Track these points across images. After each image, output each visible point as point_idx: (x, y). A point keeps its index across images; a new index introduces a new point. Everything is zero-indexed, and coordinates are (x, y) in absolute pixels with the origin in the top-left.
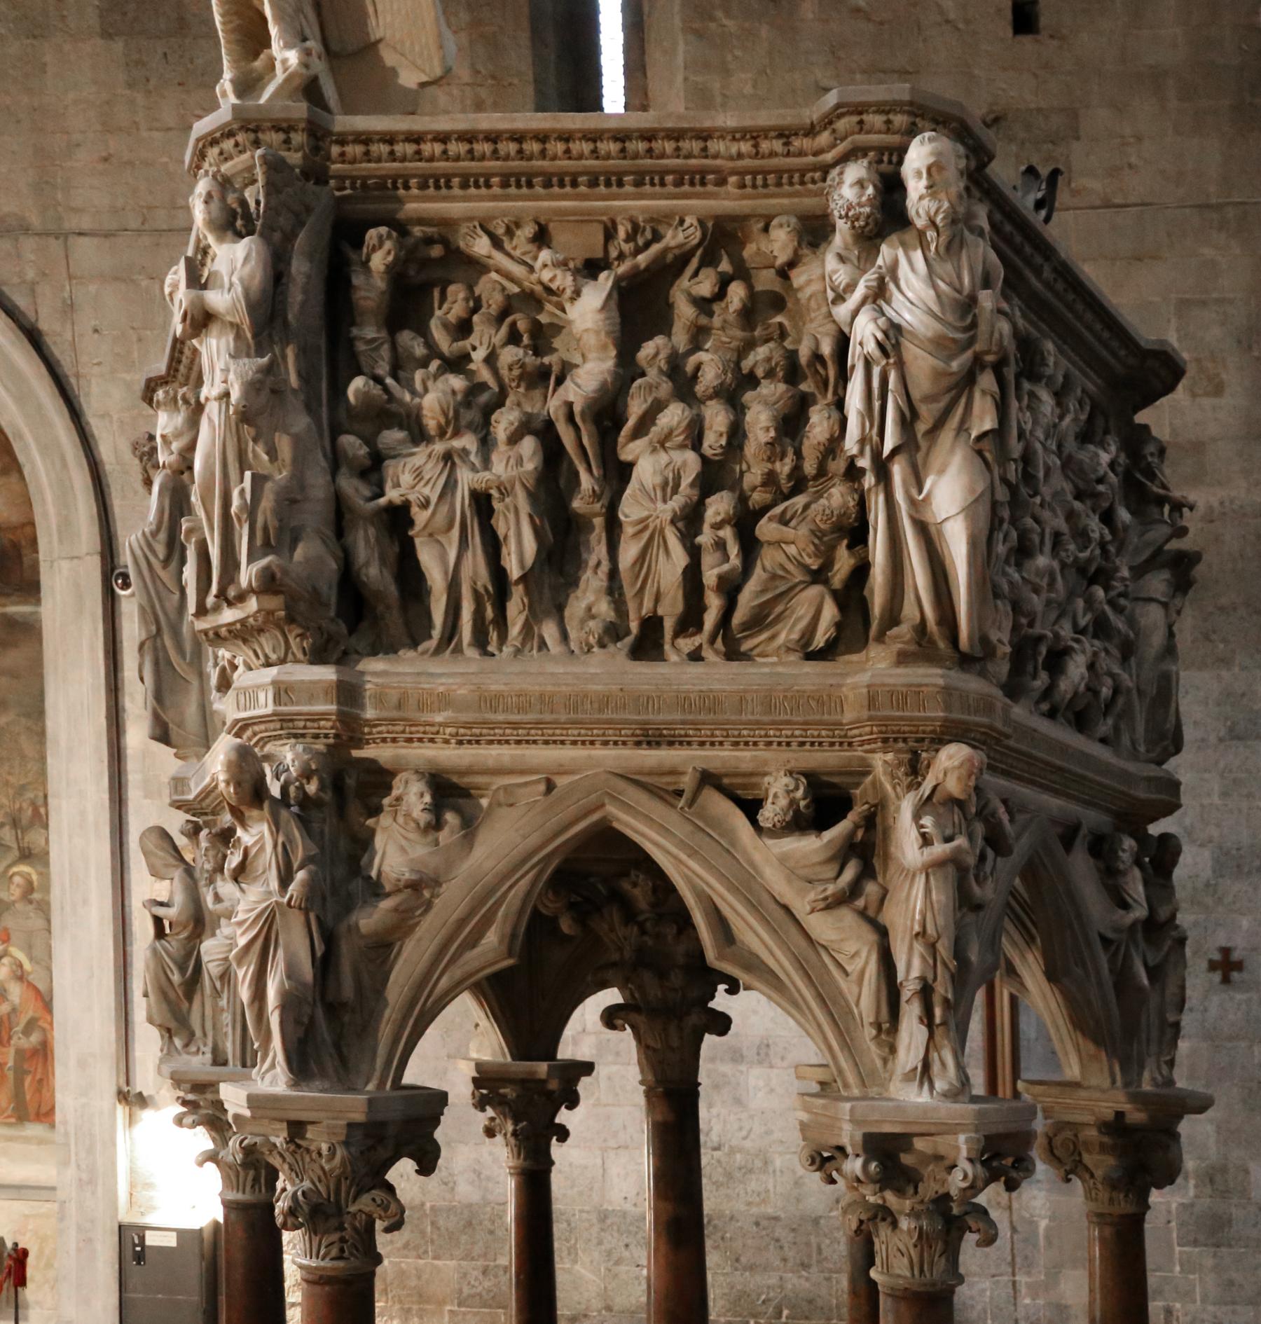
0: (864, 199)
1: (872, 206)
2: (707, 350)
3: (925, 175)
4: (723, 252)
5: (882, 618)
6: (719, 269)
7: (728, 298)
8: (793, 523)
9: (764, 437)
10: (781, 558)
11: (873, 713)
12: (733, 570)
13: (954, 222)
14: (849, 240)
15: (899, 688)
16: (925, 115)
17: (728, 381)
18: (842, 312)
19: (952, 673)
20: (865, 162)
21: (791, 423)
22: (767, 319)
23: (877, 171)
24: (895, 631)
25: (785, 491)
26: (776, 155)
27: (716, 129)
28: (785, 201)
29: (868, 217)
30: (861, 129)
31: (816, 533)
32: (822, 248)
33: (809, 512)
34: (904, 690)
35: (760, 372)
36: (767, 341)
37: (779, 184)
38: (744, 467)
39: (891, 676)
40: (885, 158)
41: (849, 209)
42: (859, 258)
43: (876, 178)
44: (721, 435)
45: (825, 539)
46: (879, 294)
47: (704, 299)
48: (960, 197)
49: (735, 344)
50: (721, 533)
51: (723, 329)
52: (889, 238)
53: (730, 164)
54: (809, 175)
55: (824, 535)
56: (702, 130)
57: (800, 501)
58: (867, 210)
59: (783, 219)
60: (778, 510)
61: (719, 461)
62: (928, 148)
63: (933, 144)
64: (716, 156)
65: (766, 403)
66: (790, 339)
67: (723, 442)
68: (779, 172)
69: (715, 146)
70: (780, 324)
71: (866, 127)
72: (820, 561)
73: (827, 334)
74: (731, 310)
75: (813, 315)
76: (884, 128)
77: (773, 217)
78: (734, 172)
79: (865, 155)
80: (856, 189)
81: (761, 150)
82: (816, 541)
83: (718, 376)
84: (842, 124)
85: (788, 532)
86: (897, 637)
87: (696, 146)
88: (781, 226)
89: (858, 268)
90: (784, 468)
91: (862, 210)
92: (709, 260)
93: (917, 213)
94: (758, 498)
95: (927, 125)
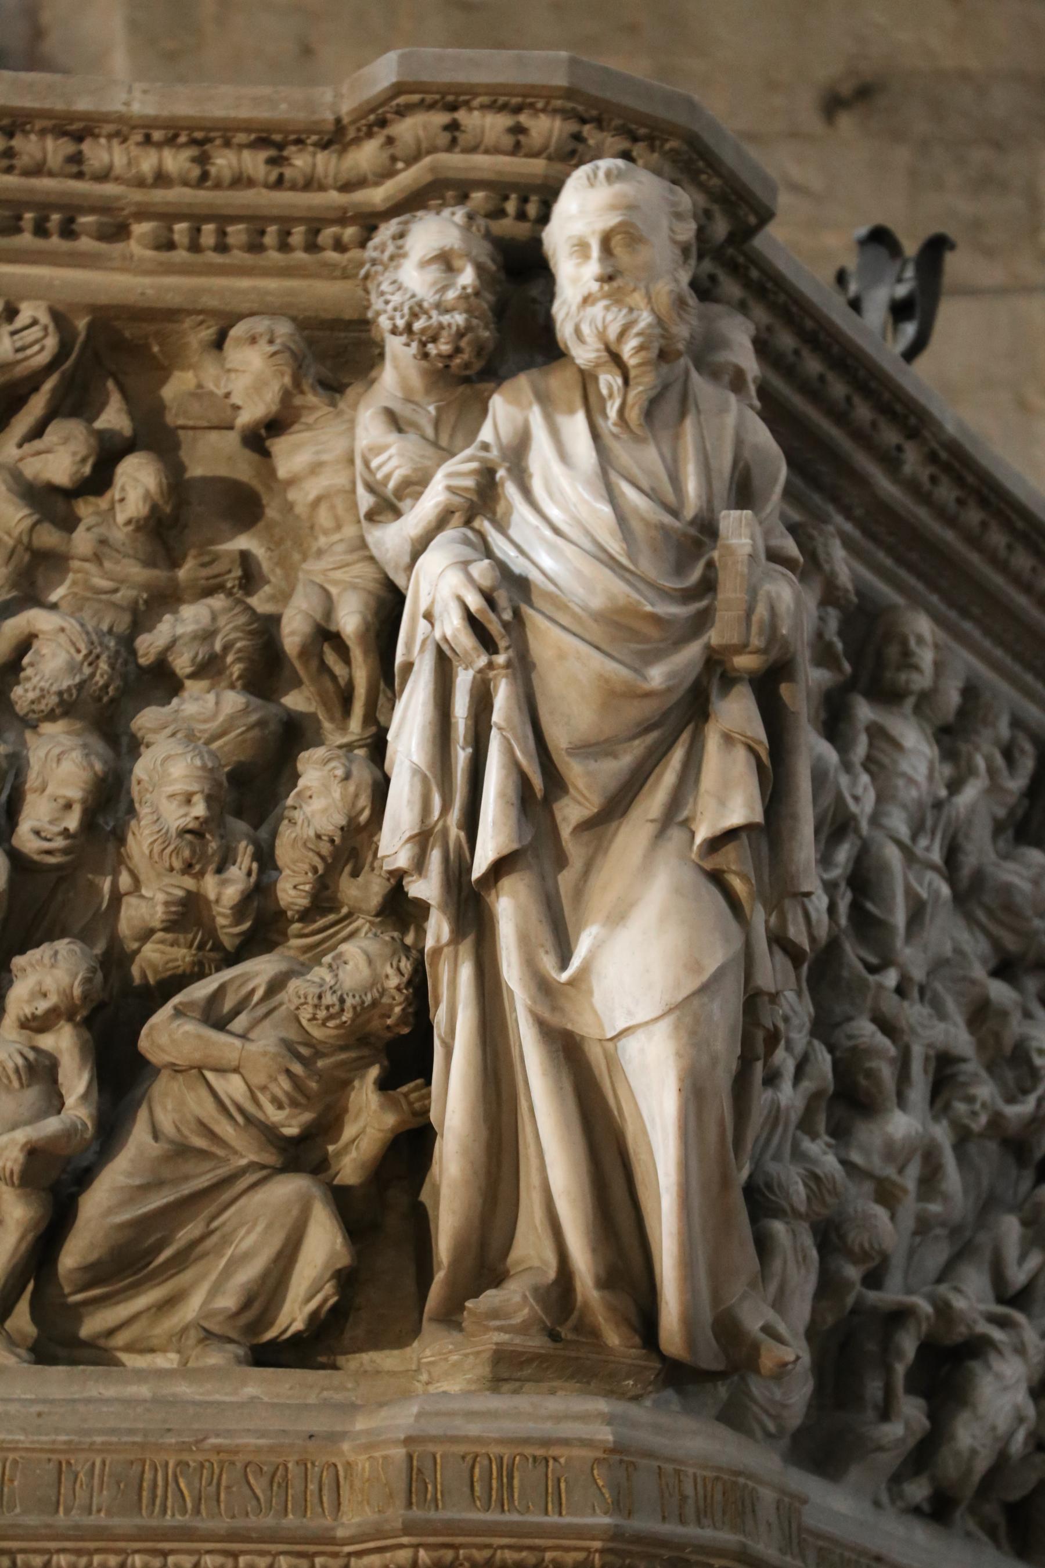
0: (451, 295)
1: (469, 311)
2: (54, 607)
3: (595, 251)
4: (110, 384)
5: (456, 1261)
6: (99, 424)
7: (115, 493)
8: (239, 1024)
9: (177, 817)
10: (208, 1110)
11: (417, 1513)
12: (70, 1133)
13: (664, 356)
14: (416, 381)
15: (494, 1450)
16: (599, 120)
17: (100, 680)
18: (391, 539)
19: (634, 1411)
20: (459, 215)
21: (251, 788)
22: (212, 542)
23: (488, 235)
24: (491, 1298)
25: (228, 943)
26: (251, 183)
27: (104, 118)
28: (272, 284)
29: (460, 334)
30: (454, 141)
31: (299, 1050)
32: (351, 392)
33: (282, 996)
34: (506, 1452)
35: (182, 663)
36: (209, 592)
37: (255, 247)
38: (125, 881)
39: (471, 1415)
40: (511, 206)
41: (414, 316)
42: (437, 424)
43: (483, 250)
44: (68, 806)
45: (320, 1064)
46: (481, 502)
47: (52, 489)
48: (680, 303)
49: (125, 595)
50: (47, 1041)
51: (97, 558)
52: (507, 385)
53: (137, 196)
54: (328, 233)
55: (318, 1054)
56: (71, 117)
57: (261, 968)
58: (459, 319)
59: (260, 325)
60: (201, 990)
61: (58, 867)
62: (603, 194)
63: (618, 187)
64: (104, 176)
65: (191, 737)
66: (267, 589)
67: (72, 822)
68: (257, 223)
69: (99, 153)
70: (245, 556)
71: (462, 139)
72: (307, 1117)
73: (354, 587)
74: (121, 518)
75: (323, 541)
76: (508, 141)
77: (241, 317)
78: (143, 214)
79: (463, 198)
80: (434, 272)
81: (213, 170)
82: (297, 1069)
83: (73, 668)
84: (409, 129)
85: (224, 1045)
86: (495, 1314)
87: (56, 150)
88: (253, 340)
89: (435, 444)
90: (223, 891)
91: (446, 319)
92: (75, 401)
93: (578, 332)
94: (154, 957)
95: (614, 142)
